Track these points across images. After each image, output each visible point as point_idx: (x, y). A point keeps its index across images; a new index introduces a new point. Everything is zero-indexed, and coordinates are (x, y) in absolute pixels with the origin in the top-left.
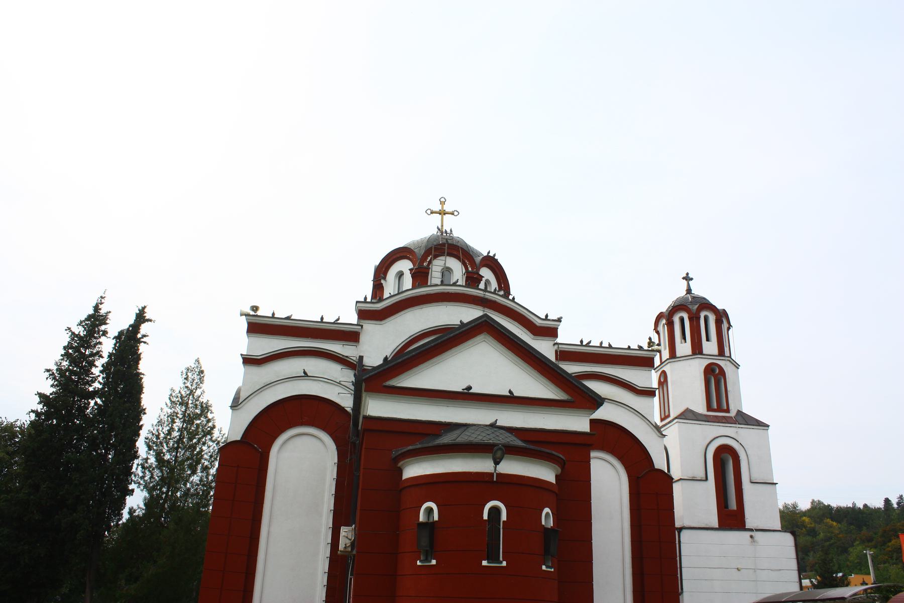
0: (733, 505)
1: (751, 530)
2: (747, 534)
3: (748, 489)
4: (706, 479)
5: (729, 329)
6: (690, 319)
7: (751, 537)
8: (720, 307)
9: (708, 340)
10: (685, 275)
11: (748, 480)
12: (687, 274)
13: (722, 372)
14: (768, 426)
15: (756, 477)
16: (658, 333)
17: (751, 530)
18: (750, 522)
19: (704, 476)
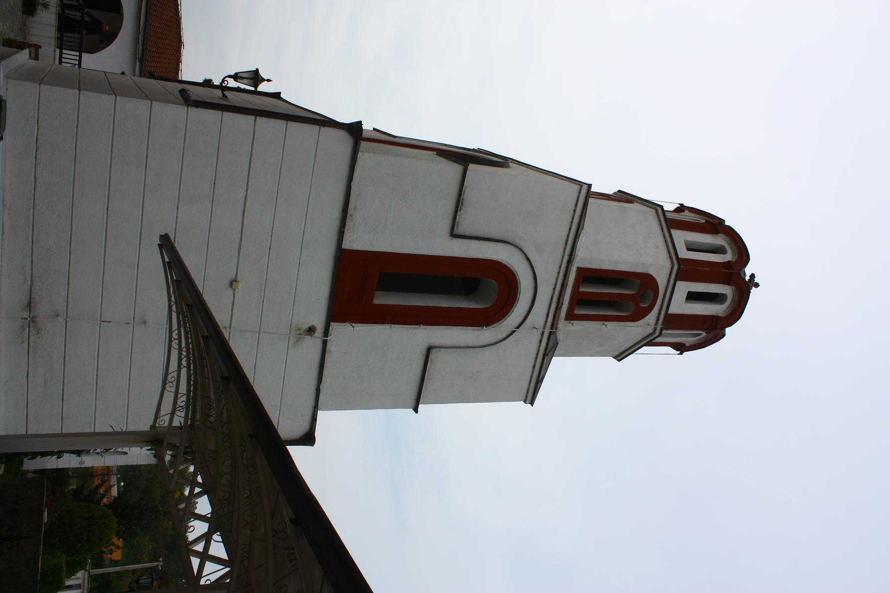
0: (382, 299)
1: (326, 333)
2: (318, 319)
3: (421, 336)
4: (454, 235)
5: (681, 348)
6: (728, 264)
7: (311, 330)
8: (728, 330)
9: (692, 297)
10: (756, 280)
11: (435, 341)
12: (757, 285)
13: (638, 315)
14: (532, 403)
15: (439, 360)
16: (681, 208)
17: (326, 333)
18: (342, 332)
19: (460, 230)
